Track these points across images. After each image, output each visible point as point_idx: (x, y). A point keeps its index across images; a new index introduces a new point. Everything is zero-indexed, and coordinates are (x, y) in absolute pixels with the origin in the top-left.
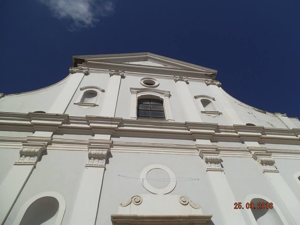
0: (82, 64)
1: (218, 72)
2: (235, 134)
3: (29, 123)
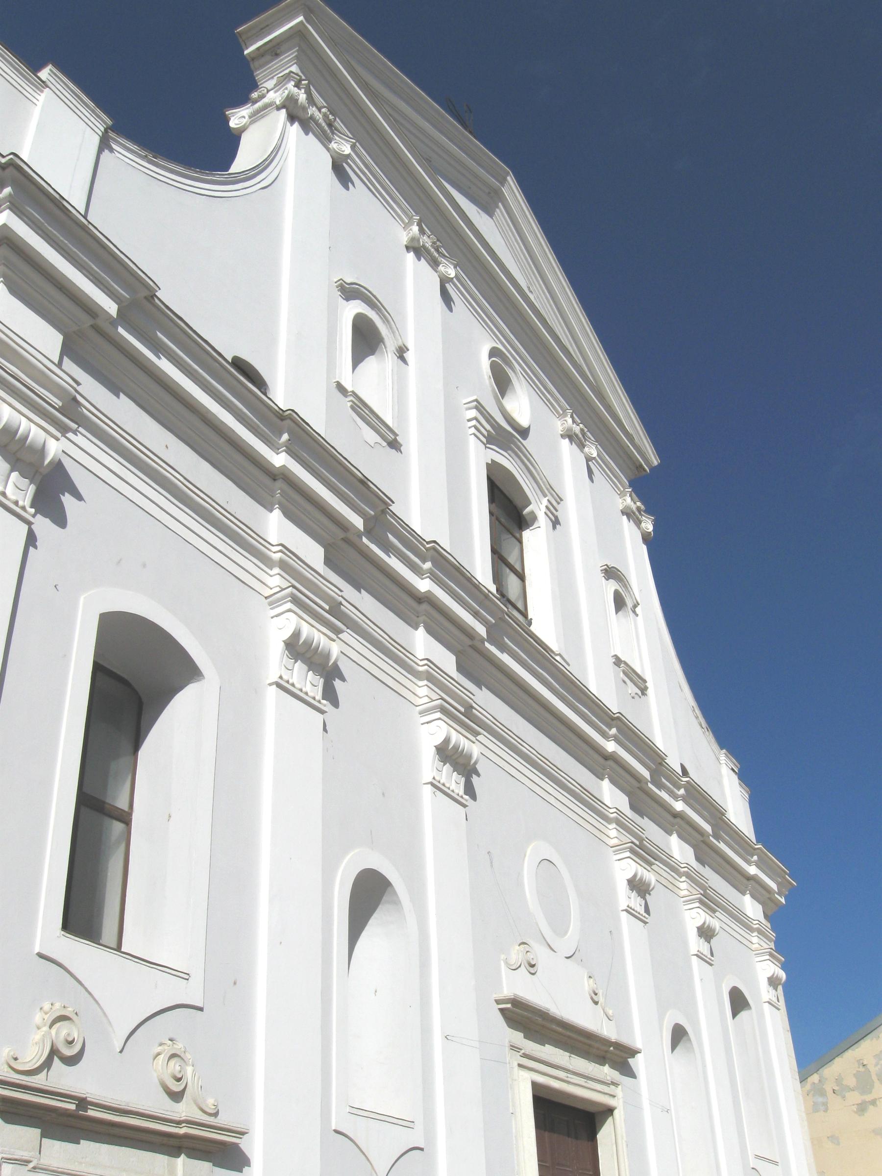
1: (659, 465)
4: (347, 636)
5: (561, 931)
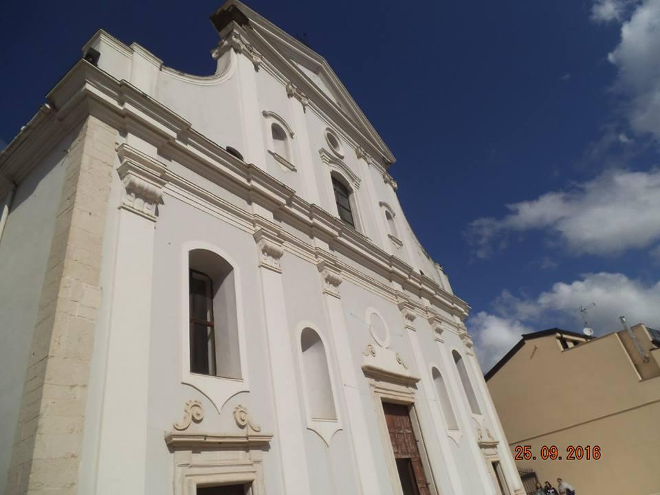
0: (241, 26)
2: (418, 285)
3: (244, 180)
4: (286, 243)
5: (383, 340)
